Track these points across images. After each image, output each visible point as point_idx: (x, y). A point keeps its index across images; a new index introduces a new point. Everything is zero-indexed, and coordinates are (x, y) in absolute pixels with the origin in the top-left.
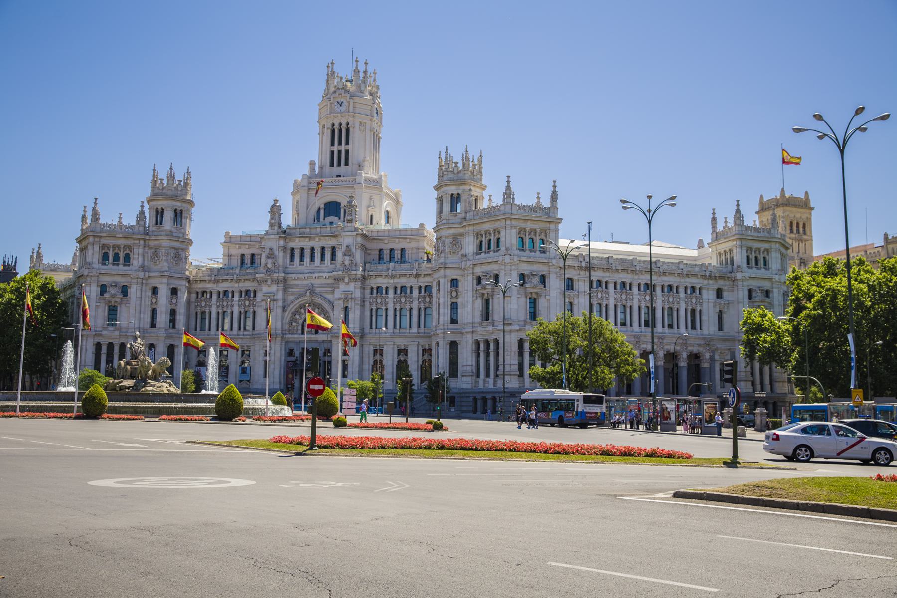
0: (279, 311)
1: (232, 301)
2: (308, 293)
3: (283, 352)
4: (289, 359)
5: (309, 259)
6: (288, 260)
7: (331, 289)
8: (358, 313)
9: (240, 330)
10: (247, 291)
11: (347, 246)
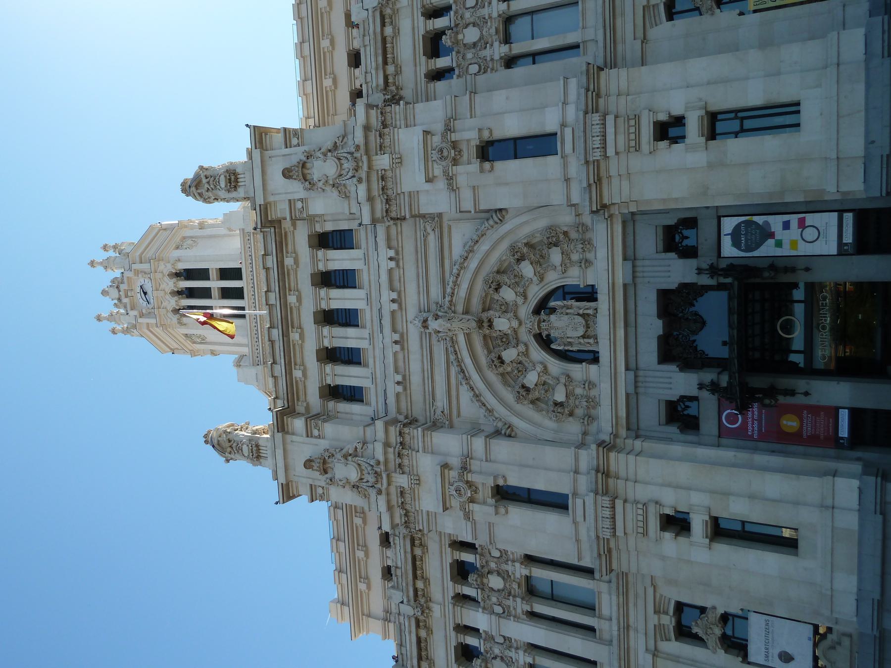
0: (502, 449)
1: (490, 638)
2: (433, 325)
3: (677, 449)
4: (709, 425)
5: (351, 331)
6: (355, 408)
7: (432, 240)
8: (499, 99)
9: (591, 629)
10: (461, 571)
11: (287, 174)
